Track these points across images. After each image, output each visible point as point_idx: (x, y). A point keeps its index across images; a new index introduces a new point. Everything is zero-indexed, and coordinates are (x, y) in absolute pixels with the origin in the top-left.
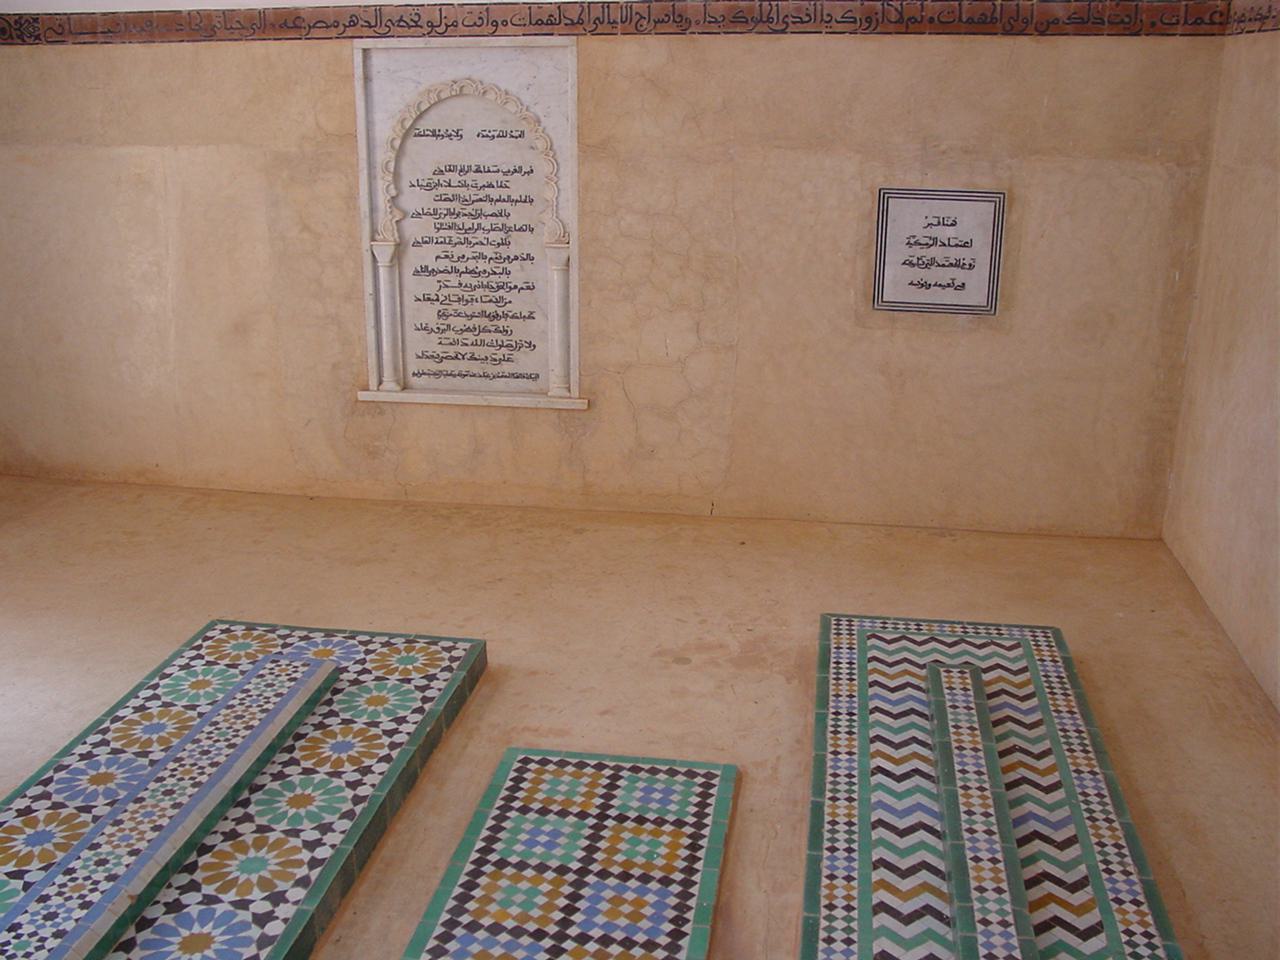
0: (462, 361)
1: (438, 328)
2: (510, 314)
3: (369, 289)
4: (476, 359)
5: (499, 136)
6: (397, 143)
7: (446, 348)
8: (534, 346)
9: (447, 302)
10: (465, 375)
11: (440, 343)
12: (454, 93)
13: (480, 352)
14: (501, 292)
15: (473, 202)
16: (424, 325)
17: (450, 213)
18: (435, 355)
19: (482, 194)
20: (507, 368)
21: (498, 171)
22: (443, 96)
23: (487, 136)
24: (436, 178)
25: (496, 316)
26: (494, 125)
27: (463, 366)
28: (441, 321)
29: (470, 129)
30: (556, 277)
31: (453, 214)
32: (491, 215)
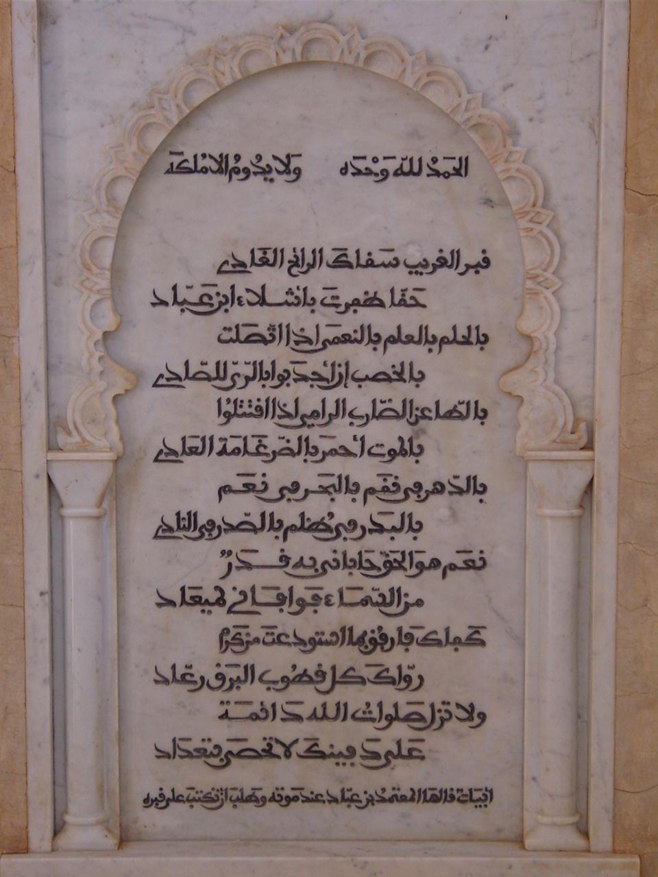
0: (284, 761)
1: (220, 676)
2: (420, 634)
3: (38, 579)
4: (322, 755)
5: (399, 172)
6: (123, 191)
7: (238, 729)
8: (483, 716)
9: (247, 606)
10: (290, 800)
11: (225, 716)
12: (287, 59)
13: (334, 735)
14: (396, 579)
15: (326, 343)
16: (180, 671)
17: (260, 373)
18: (209, 747)
19: (349, 323)
20: (405, 775)
21: (395, 264)
23: (369, 172)
24: (224, 284)
25: (380, 641)
26: (387, 142)
27: (286, 774)
28: (229, 657)
29: (320, 153)
30: (554, 543)
31: (271, 375)
32: (375, 379)
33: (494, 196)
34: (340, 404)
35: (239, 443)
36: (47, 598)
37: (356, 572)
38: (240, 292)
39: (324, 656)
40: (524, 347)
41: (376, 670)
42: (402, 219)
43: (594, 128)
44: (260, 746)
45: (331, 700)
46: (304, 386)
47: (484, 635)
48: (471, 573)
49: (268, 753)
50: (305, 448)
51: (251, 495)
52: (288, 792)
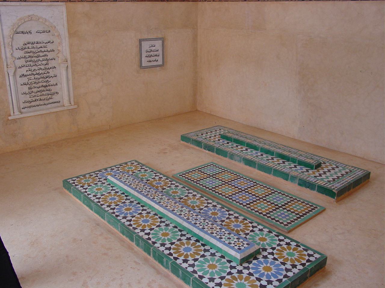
0: (37, 101)
1: (29, 93)
2: (50, 85)
3: (8, 84)
4: (41, 100)
5: (43, 32)
6: (11, 36)
7: (32, 99)
8: (58, 93)
9: (31, 84)
10: (39, 106)
11: (30, 97)
13: (42, 98)
14: (47, 79)
15: (37, 53)
16: (24, 93)
17: (29, 57)
18: (29, 101)
19: (39, 50)
20: (51, 101)
21: (43, 43)
22: (26, 20)
23: (39, 32)
24: (24, 46)
25: (46, 86)
26: (41, 29)
27: (38, 103)
28: (30, 90)
29: (33, 30)
30: (64, 73)
31: (31, 57)
32: (43, 56)
33: (53, 34)
34: (39, 59)
35: (28, 65)
36: (9, 86)
37: (43, 79)
38: (26, 47)
39: (40, 89)
40: (58, 51)
41: (46, 90)
42: (43, 38)
43: (64, 26)
44: (35, 100)
45: (42, 94)
46: (35, 58)
47: (57, 84)
48: (55, 77)
49: (35, 101)
50: (36, 65)
51: (30, 71)
52: (38, 105)
